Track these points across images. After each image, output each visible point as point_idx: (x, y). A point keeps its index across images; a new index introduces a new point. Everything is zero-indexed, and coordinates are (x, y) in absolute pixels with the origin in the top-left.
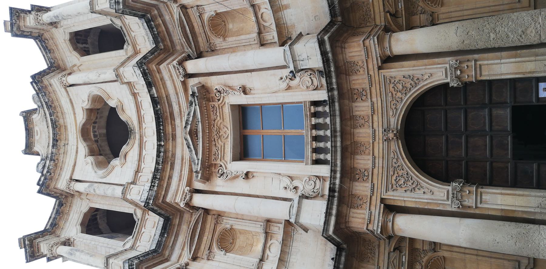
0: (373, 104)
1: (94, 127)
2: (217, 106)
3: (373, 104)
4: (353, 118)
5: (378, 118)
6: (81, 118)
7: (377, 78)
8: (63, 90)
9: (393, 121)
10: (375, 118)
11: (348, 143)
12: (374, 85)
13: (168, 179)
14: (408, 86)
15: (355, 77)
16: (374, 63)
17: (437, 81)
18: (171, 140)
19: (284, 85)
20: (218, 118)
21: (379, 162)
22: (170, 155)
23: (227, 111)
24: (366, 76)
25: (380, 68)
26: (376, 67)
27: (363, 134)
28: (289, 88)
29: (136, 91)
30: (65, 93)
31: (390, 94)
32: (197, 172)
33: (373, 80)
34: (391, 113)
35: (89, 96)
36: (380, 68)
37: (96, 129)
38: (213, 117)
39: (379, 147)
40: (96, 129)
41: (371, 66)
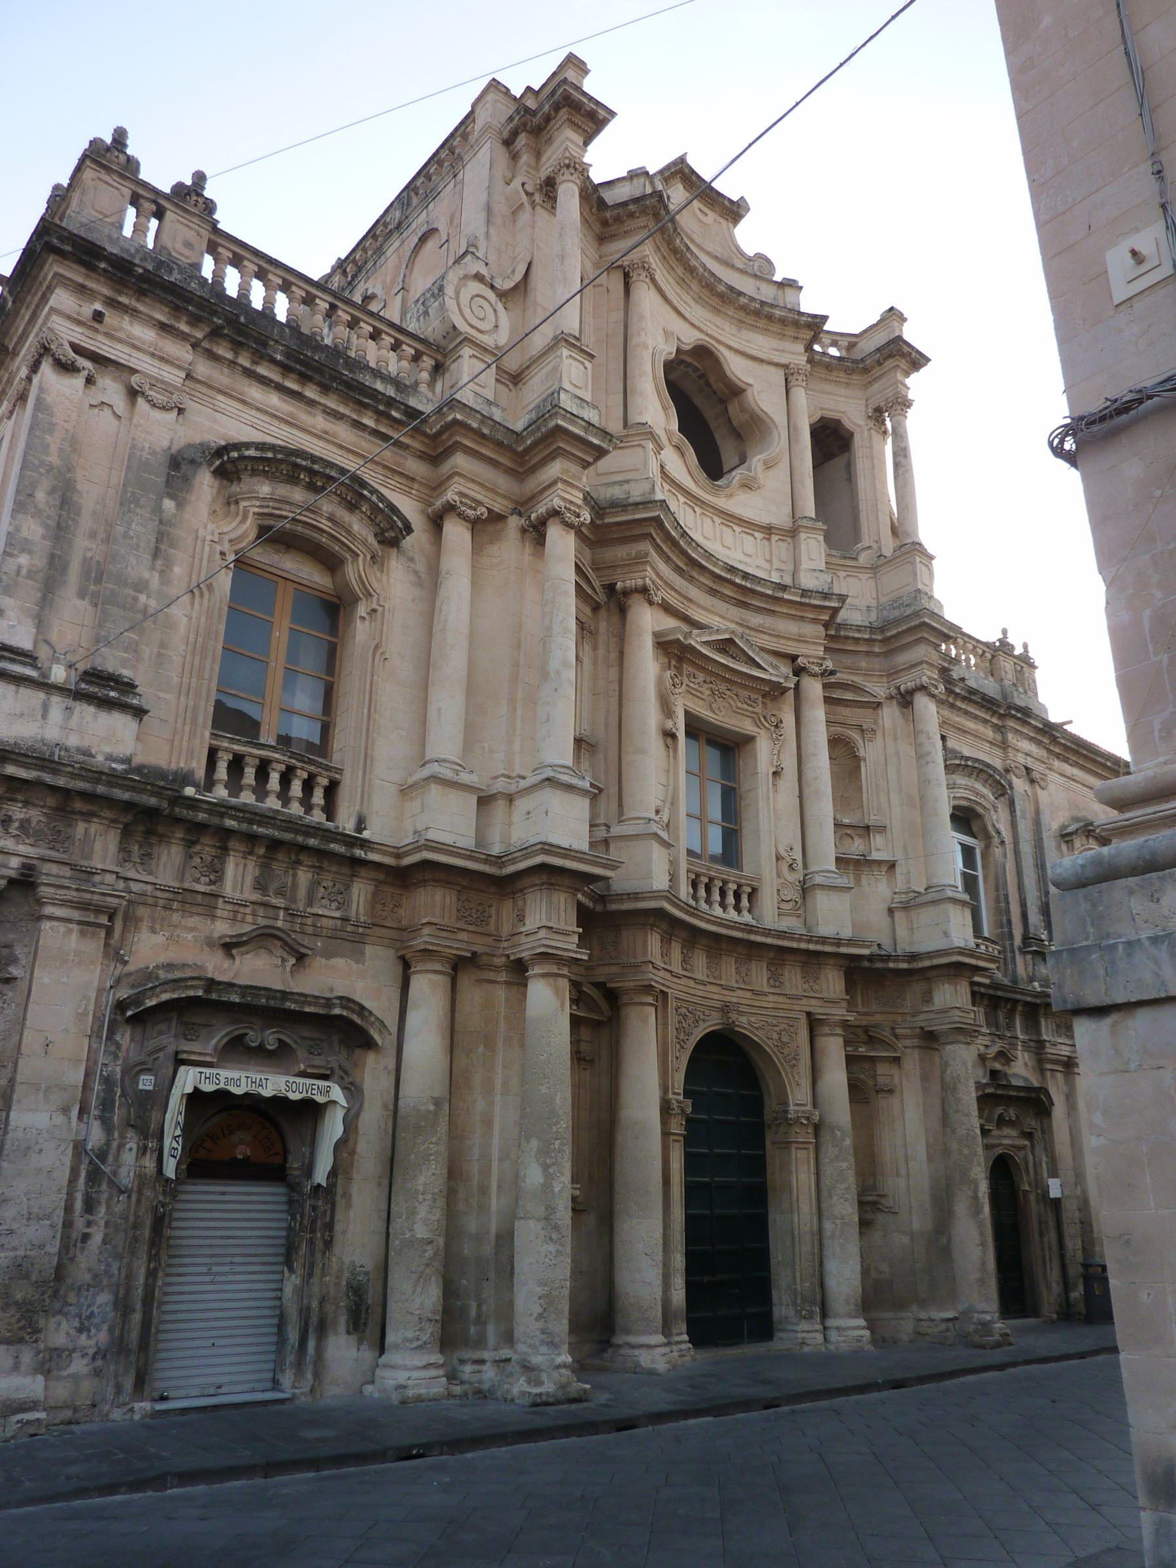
0: (765, 994)
1: (696, 369)
2: (756, 710)
3: (765, 994)
4: (749, 957)
5: (763, 1007)
6: (737, 368)
7: (796, 1008)
8: (783, 361)
9: (744, 1019)
10: (748, 995)
11: (724, 946)
12: (789, 1001)
13: (668, 557)
14: (786, 1051)
15: (799, 976)
16: (818, 1009)
17: (792, 1091)
18: (711, 584)
19: (783, 853)
20: (739, 704)
21: (700, 990)
22: (694, 574)
23: (747, 726)
24: (800, 992)
25: (809, 1014)
26: (811, 1010)
27: (729, 969)
28: (779, 858)
29: (774, 538)
30: (776, 360)
31: (775, 1022)
32: (687, 635)
33: (796, 1002)
34: (753, 1019)
35: (774, 423)
36: (809, 1014)
37: (690, 370)
38: (744, 693)
39: (716, 994)
40: (690, 370)
41: (813, 1002)
